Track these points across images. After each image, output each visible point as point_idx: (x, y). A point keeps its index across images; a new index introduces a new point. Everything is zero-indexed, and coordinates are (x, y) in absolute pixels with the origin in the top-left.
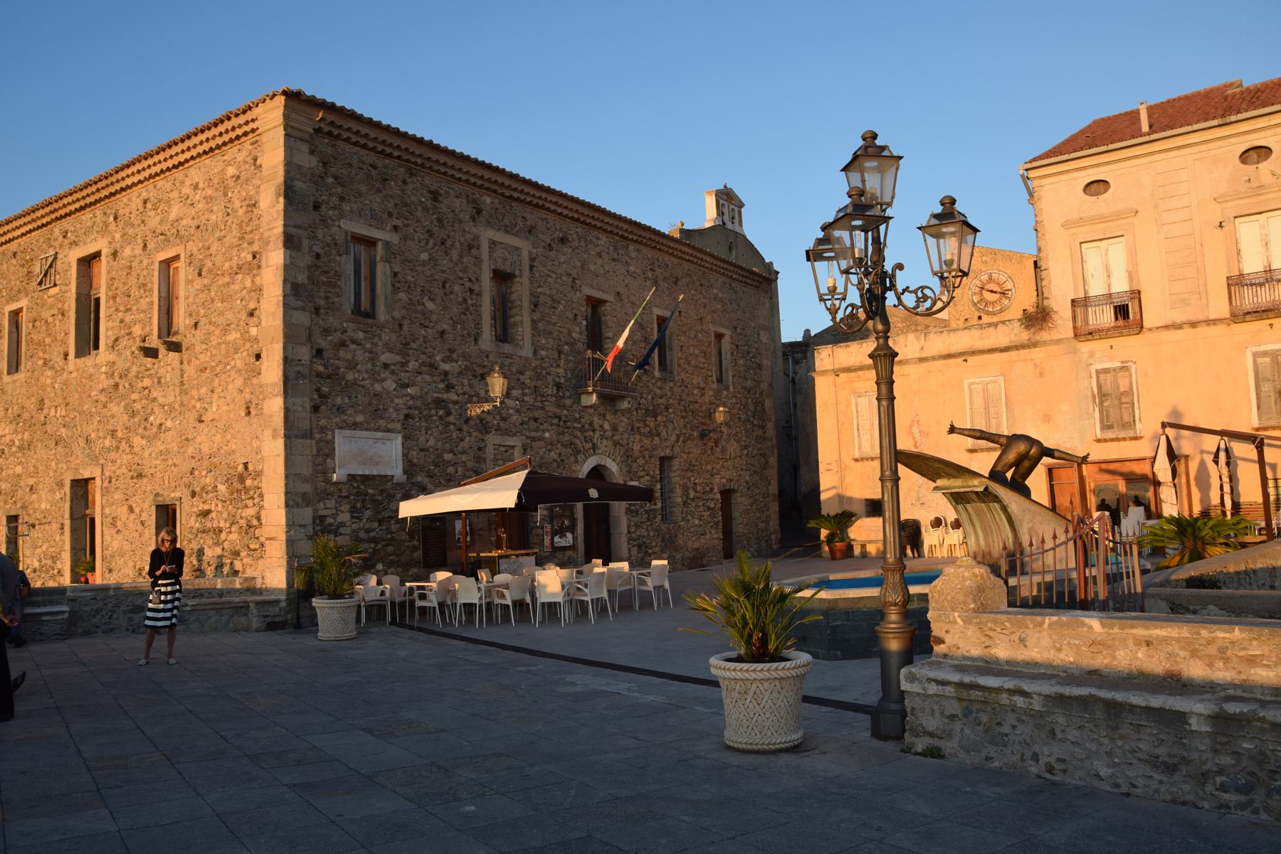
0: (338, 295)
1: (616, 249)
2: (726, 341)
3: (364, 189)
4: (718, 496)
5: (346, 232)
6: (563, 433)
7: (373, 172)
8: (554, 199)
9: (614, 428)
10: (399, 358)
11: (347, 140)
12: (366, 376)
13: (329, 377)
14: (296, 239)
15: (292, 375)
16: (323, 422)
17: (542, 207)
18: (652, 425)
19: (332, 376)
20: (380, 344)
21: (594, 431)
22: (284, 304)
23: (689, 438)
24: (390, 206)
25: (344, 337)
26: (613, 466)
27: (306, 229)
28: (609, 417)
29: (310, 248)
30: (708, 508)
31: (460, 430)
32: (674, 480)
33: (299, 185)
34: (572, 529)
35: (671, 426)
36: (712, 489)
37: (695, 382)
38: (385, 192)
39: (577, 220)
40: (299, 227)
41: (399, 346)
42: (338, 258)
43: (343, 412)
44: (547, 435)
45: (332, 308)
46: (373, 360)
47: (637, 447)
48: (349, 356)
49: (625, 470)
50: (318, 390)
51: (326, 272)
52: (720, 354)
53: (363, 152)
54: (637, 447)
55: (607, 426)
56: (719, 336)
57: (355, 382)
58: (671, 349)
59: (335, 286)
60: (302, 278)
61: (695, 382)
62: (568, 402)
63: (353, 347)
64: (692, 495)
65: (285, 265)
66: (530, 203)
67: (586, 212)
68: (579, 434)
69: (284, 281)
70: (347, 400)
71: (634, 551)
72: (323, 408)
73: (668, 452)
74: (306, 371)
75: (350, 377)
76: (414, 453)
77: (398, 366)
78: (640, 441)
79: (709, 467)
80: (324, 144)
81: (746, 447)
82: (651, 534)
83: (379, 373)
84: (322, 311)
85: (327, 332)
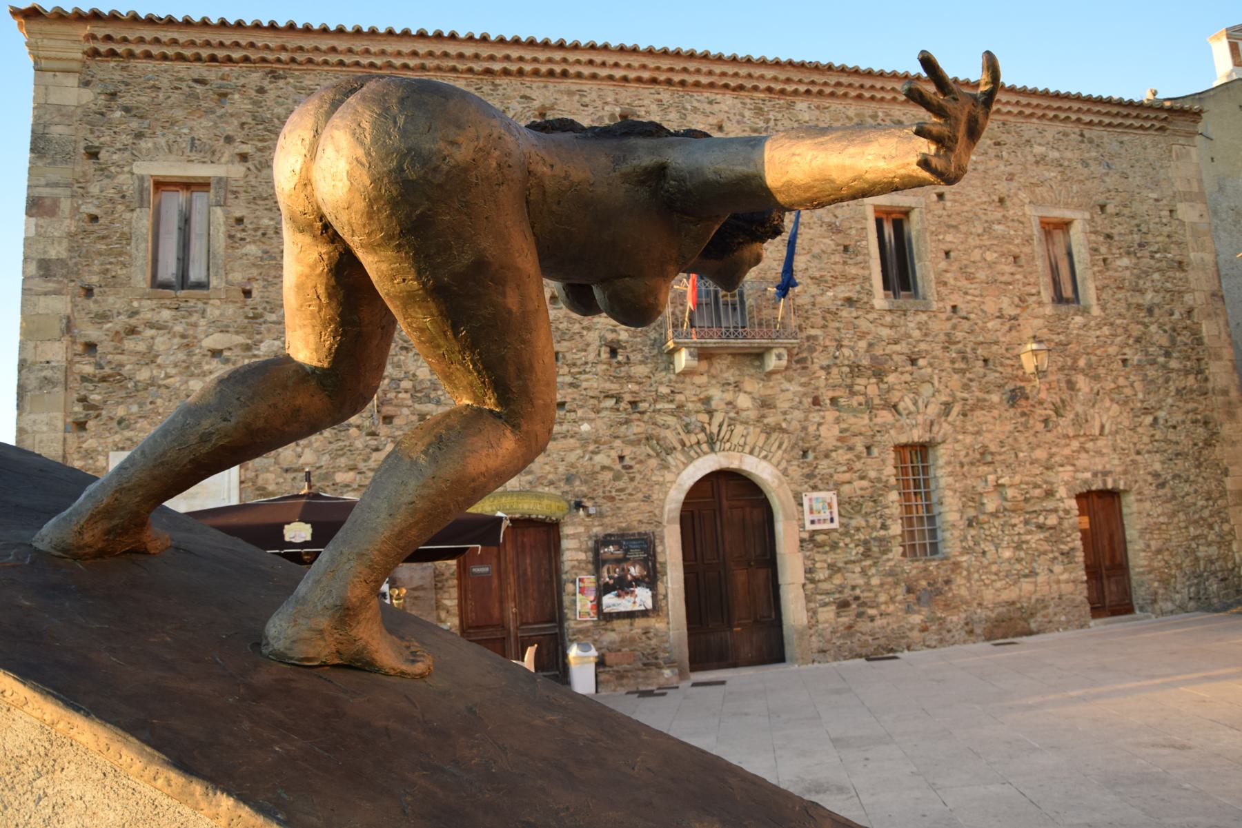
0: (124, 265)
1: (759, 111)
2: (1077, 235)
3: (179, 114)
4: (1073, 504)
5: (142, 179)
6: (627, 422)
7: (199, 88)
8: (584, 57)
9: (765, 404)
10: (240, 339)
11: (148, 55)
12: (172, 371)
13: (104, 379)
14: (48, 202)
15: (32, 383)
16: (91, 443)
17: (565, 74)
18: (872, 390)
19: (112, 379)
20: (202, 322)
21: (711, 413)
22: (24, 290)
23: (980, 404)
24: (231, 128)
25: (133, 321)
26: (762, 470)
27: (68, 186)
28: (749, 385)
29: (76, 210)
30: (1040, 527)
31: (373, 434)
32: (943, 482)
33: (56, 131)
34: (651, 579)
35: (926, 390)
36: (1050, 494)
37: (990, 306)
38: (220, 112)
39: (654, 81)
40: (57, 185)
41: (241, 321)
42: (128, 215)
43: (128, 427)
44: (585, 427)
45: (113, 283)
46: (188, 345)
47: (829, 434)
48: (142, 347)
49: (795, 471)
50: (83, 399)
51: (103, 238)
52: (1070, 255)
53: (180, 66)
54: (829, 434)
55: (743, 401)
56: (1055, 228)
57: (152, 382)
58: (920, 260)
59: (120, 254)
60: (56, 251)
61: (990, 306)
62: (640, 370)
63: (149, 333)
64: (991, 505)
65: (26, 239)
66: (536, 73)
67: (665, 64)
68: (671, 420)
69: (26, 259)
70: (135, 409)
71: (827, 614)
72: (91, 424)
73: (917, 435)
74: (59, 376)
75: (144, 375)
76: (271, 476)
77: (237, 351)
78: (838, 421)
79: (1040, 454)
80: (109, 71)
81: (1146, 411)
82: (875, 581)
83: (199, 365)
84: (96, 291)
85: (102, 318)
